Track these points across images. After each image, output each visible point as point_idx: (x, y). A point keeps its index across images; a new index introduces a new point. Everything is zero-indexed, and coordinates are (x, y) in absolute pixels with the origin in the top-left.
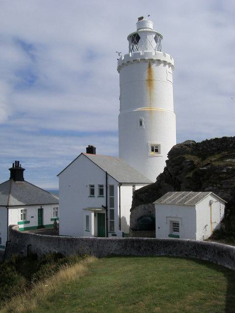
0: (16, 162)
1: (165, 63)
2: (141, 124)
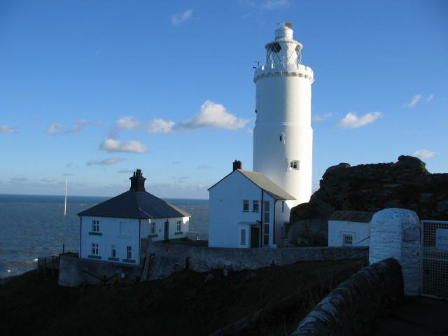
0: (137, 170)
1: (300, 75)
2: (281, 140)
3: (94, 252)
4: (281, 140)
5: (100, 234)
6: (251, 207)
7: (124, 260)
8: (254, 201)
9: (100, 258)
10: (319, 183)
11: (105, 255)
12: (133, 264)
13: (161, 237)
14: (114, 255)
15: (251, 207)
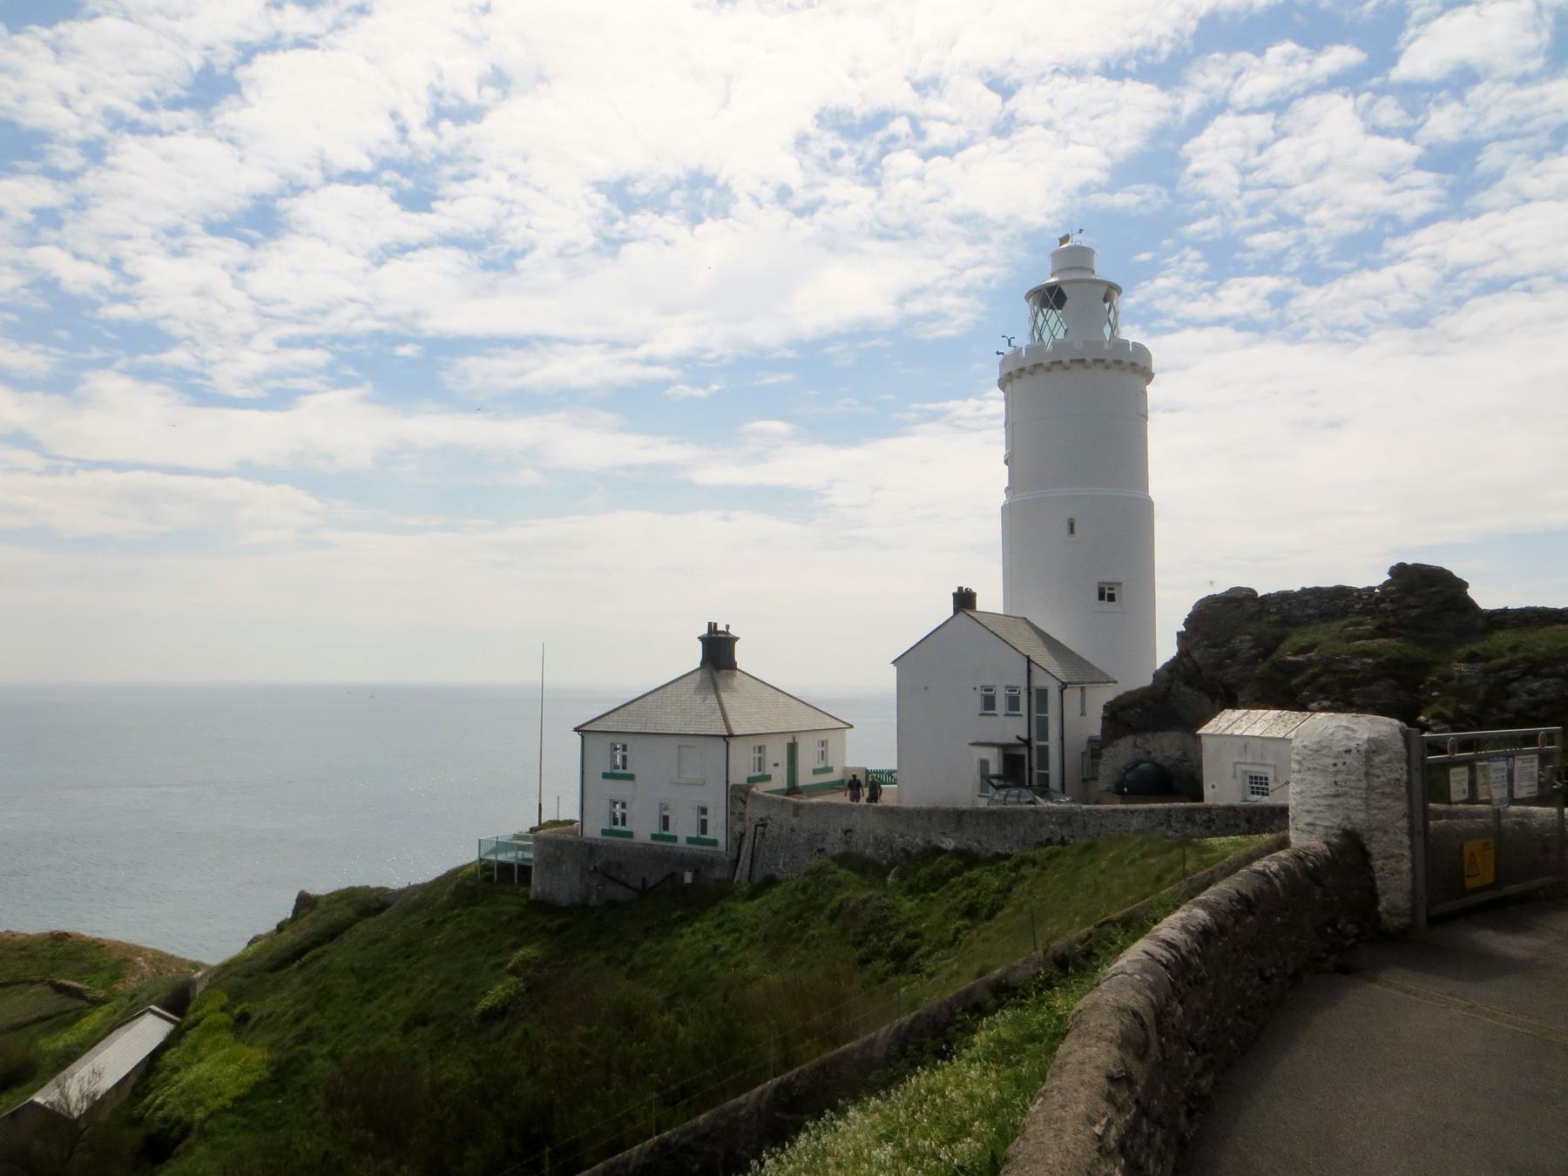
2: (1072, 531)
3: (616, 822)
4: (1072, 531)
5: (631, 777)
7: (690, 840)
8: (1012, 689)
9: (630, 835)
11: (643, 828)
13: (779, 781)
14: (666, 827)
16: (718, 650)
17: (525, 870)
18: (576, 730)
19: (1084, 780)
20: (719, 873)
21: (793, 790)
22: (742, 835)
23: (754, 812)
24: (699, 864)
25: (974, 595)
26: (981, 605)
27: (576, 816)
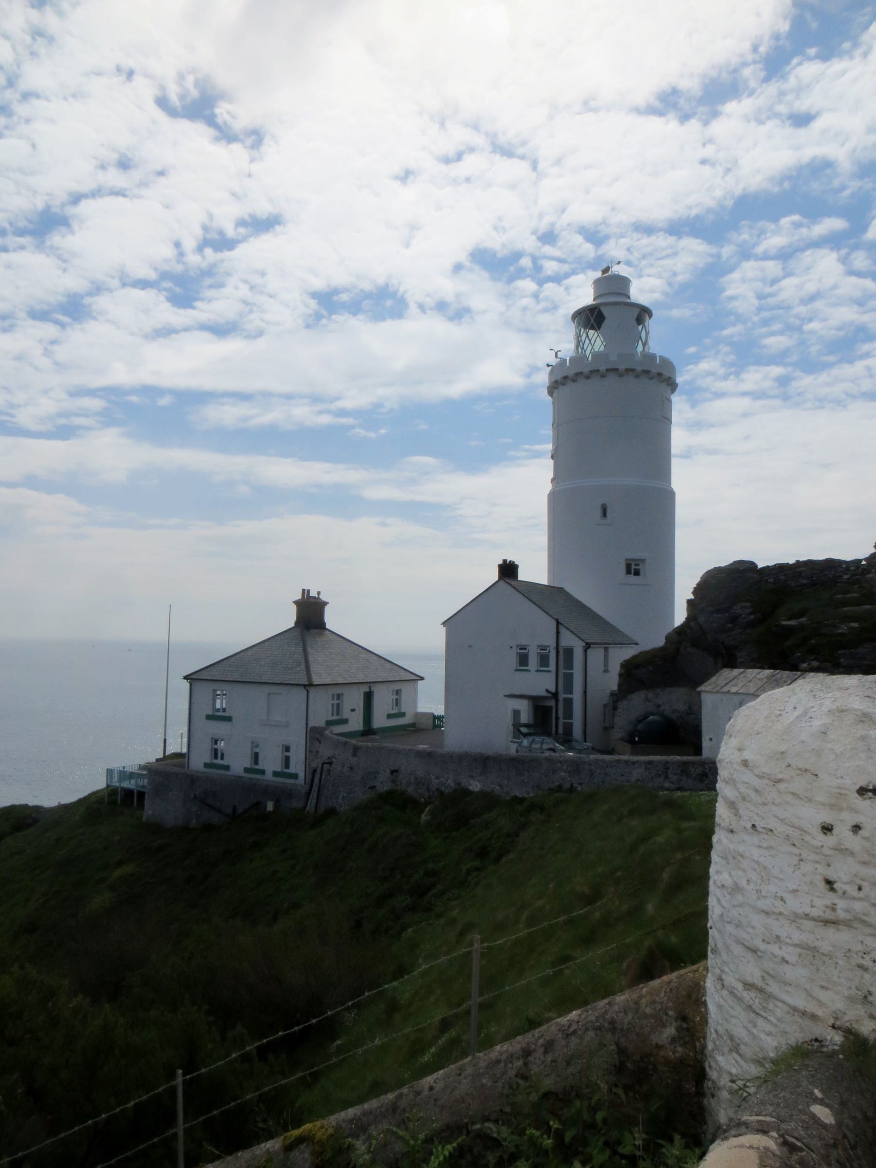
3: (216, 757)
5: (229, 719)
6: (533, 662)
7: (276, 774)
8: (543, 648)
9: (227, 768)
10: (685, 605)
11: (238, 763)
12: (292, 781)
13: (356, 723)
15: (533, 662)
16: (310, 613)
17: (141, 795)
18: (186, 678)
19: (606, 729)
20: (296, 804)
21: (368, 731)
22: (315, 771)
23: (325, 751)
24: (280, 794)
25: (517, 566)
26: (522, 576)
27: (185, 750)
